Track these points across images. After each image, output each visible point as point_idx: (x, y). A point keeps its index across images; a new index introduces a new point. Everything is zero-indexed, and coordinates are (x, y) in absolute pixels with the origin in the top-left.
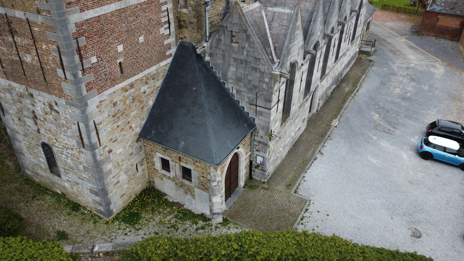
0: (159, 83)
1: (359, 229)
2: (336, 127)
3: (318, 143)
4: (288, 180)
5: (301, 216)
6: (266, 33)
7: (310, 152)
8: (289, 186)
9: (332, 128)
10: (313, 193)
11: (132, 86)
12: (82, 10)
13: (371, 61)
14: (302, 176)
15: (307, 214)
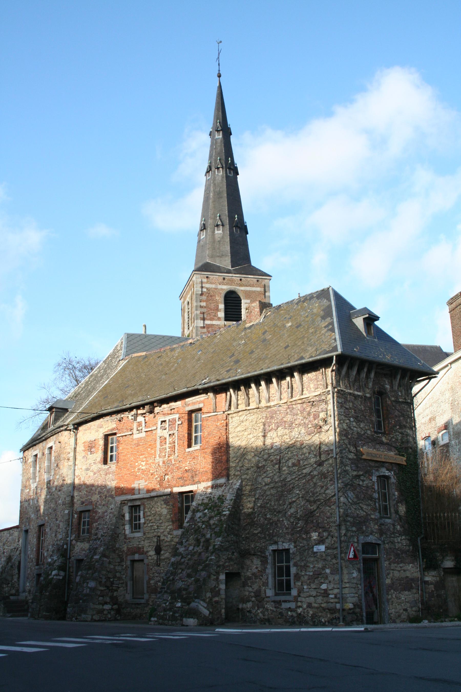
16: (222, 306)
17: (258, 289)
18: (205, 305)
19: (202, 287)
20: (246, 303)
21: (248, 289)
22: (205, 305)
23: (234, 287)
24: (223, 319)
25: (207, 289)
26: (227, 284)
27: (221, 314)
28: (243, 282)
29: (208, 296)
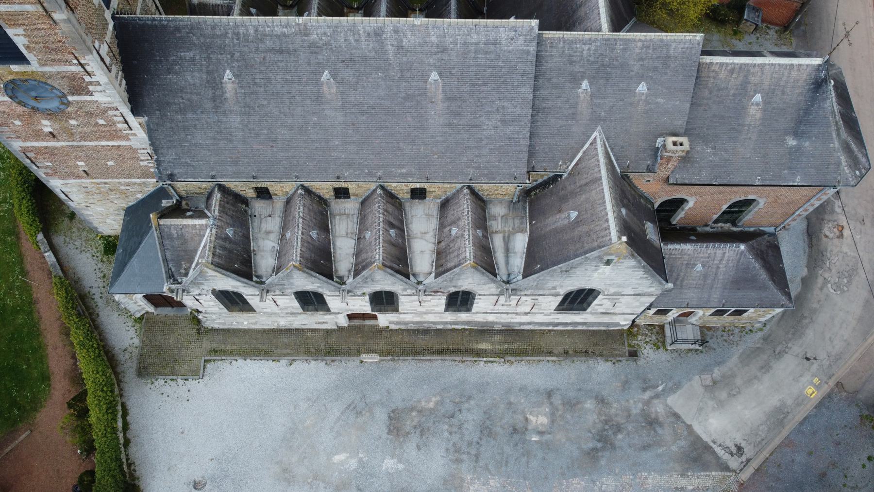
0: (151, 189)
1: (182, 433)
2: (362, 362)
3: (308, 353)
4: (223, 347)
5: (174, 377)
6: (196, 251)
7: (285, 351)
8: (215, 351)
9: (355, 358)
10: (216, 376)
11: (106, 183)
13: (633, 354)
14: (236, 358)
15: (180, 382)
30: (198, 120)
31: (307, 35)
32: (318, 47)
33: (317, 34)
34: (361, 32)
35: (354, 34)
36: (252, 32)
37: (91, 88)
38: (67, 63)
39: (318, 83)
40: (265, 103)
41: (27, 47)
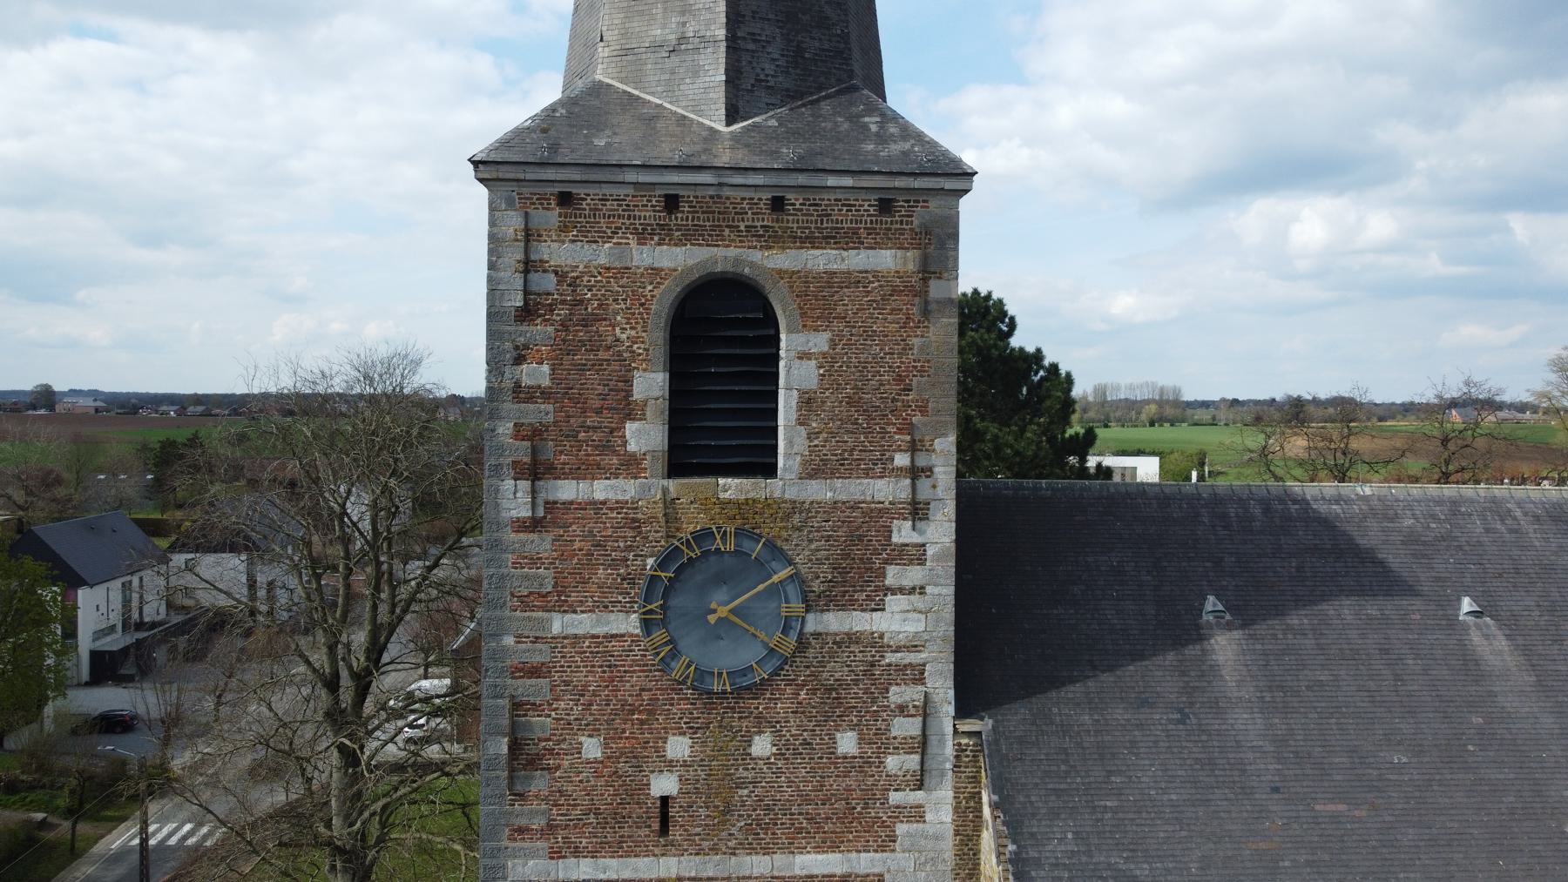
12: (556, 855)
16: (651, 384)
17: (886, 259)
18: (546, 382)
19: (528, 266)
20: (804, 356)
21: (821, 259)
22: (546, 382)
23: (732, 252)
24: (661, 466)
25: (561, 275)
26: (690, 236)
27: (646, 436)
28: (792, 222)
29: (564, 325)
30: (1140, 726)
31: (1392, 520)
32: (1425, 543)
33: (1414, 516)
34: (1518, 513)
35: (1502, 520)
36: (1257, 511)
37: (893, 575)
38: (881, 467)
39: (1452, 623)
40: (1324, 676)
41: (807, 402)
